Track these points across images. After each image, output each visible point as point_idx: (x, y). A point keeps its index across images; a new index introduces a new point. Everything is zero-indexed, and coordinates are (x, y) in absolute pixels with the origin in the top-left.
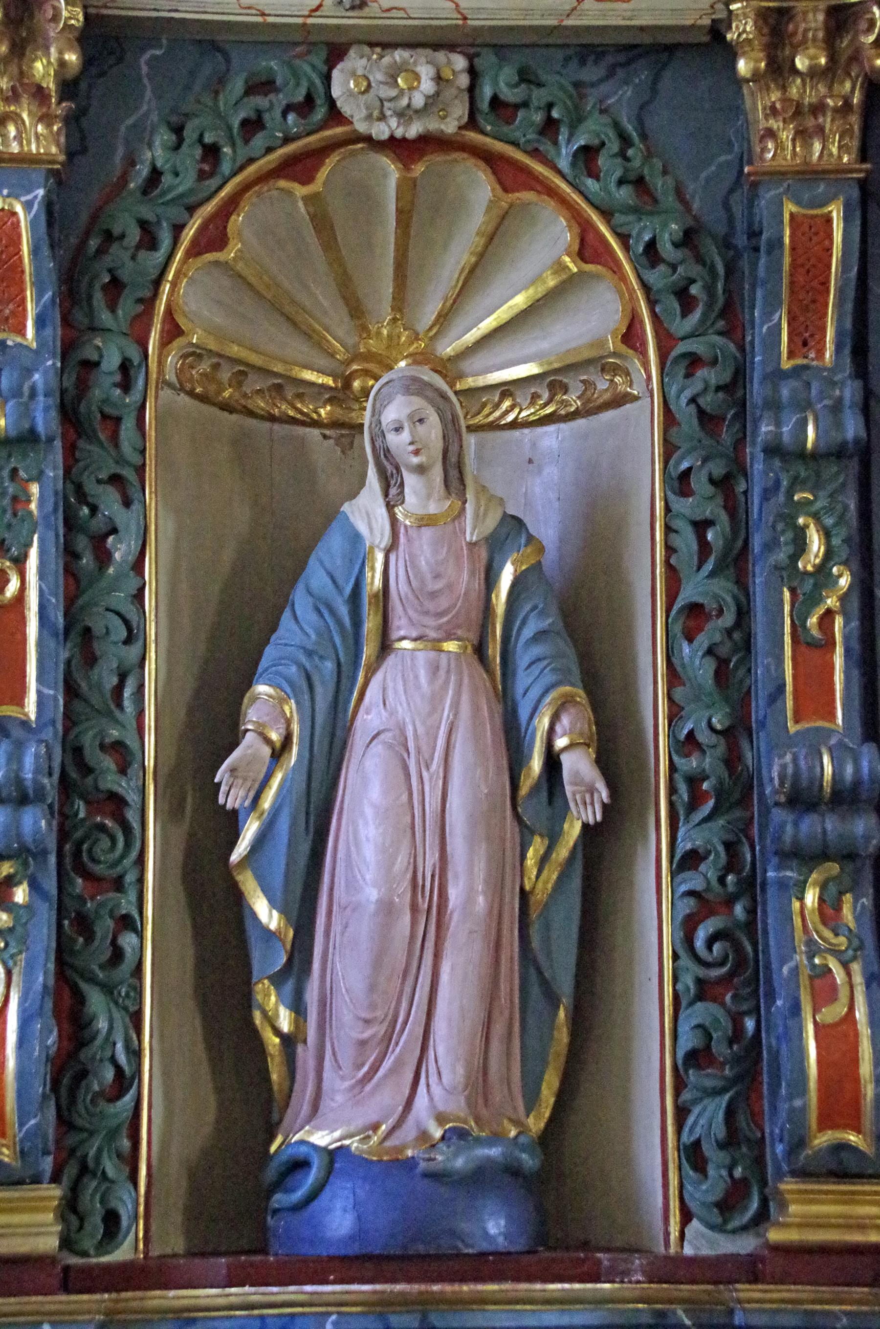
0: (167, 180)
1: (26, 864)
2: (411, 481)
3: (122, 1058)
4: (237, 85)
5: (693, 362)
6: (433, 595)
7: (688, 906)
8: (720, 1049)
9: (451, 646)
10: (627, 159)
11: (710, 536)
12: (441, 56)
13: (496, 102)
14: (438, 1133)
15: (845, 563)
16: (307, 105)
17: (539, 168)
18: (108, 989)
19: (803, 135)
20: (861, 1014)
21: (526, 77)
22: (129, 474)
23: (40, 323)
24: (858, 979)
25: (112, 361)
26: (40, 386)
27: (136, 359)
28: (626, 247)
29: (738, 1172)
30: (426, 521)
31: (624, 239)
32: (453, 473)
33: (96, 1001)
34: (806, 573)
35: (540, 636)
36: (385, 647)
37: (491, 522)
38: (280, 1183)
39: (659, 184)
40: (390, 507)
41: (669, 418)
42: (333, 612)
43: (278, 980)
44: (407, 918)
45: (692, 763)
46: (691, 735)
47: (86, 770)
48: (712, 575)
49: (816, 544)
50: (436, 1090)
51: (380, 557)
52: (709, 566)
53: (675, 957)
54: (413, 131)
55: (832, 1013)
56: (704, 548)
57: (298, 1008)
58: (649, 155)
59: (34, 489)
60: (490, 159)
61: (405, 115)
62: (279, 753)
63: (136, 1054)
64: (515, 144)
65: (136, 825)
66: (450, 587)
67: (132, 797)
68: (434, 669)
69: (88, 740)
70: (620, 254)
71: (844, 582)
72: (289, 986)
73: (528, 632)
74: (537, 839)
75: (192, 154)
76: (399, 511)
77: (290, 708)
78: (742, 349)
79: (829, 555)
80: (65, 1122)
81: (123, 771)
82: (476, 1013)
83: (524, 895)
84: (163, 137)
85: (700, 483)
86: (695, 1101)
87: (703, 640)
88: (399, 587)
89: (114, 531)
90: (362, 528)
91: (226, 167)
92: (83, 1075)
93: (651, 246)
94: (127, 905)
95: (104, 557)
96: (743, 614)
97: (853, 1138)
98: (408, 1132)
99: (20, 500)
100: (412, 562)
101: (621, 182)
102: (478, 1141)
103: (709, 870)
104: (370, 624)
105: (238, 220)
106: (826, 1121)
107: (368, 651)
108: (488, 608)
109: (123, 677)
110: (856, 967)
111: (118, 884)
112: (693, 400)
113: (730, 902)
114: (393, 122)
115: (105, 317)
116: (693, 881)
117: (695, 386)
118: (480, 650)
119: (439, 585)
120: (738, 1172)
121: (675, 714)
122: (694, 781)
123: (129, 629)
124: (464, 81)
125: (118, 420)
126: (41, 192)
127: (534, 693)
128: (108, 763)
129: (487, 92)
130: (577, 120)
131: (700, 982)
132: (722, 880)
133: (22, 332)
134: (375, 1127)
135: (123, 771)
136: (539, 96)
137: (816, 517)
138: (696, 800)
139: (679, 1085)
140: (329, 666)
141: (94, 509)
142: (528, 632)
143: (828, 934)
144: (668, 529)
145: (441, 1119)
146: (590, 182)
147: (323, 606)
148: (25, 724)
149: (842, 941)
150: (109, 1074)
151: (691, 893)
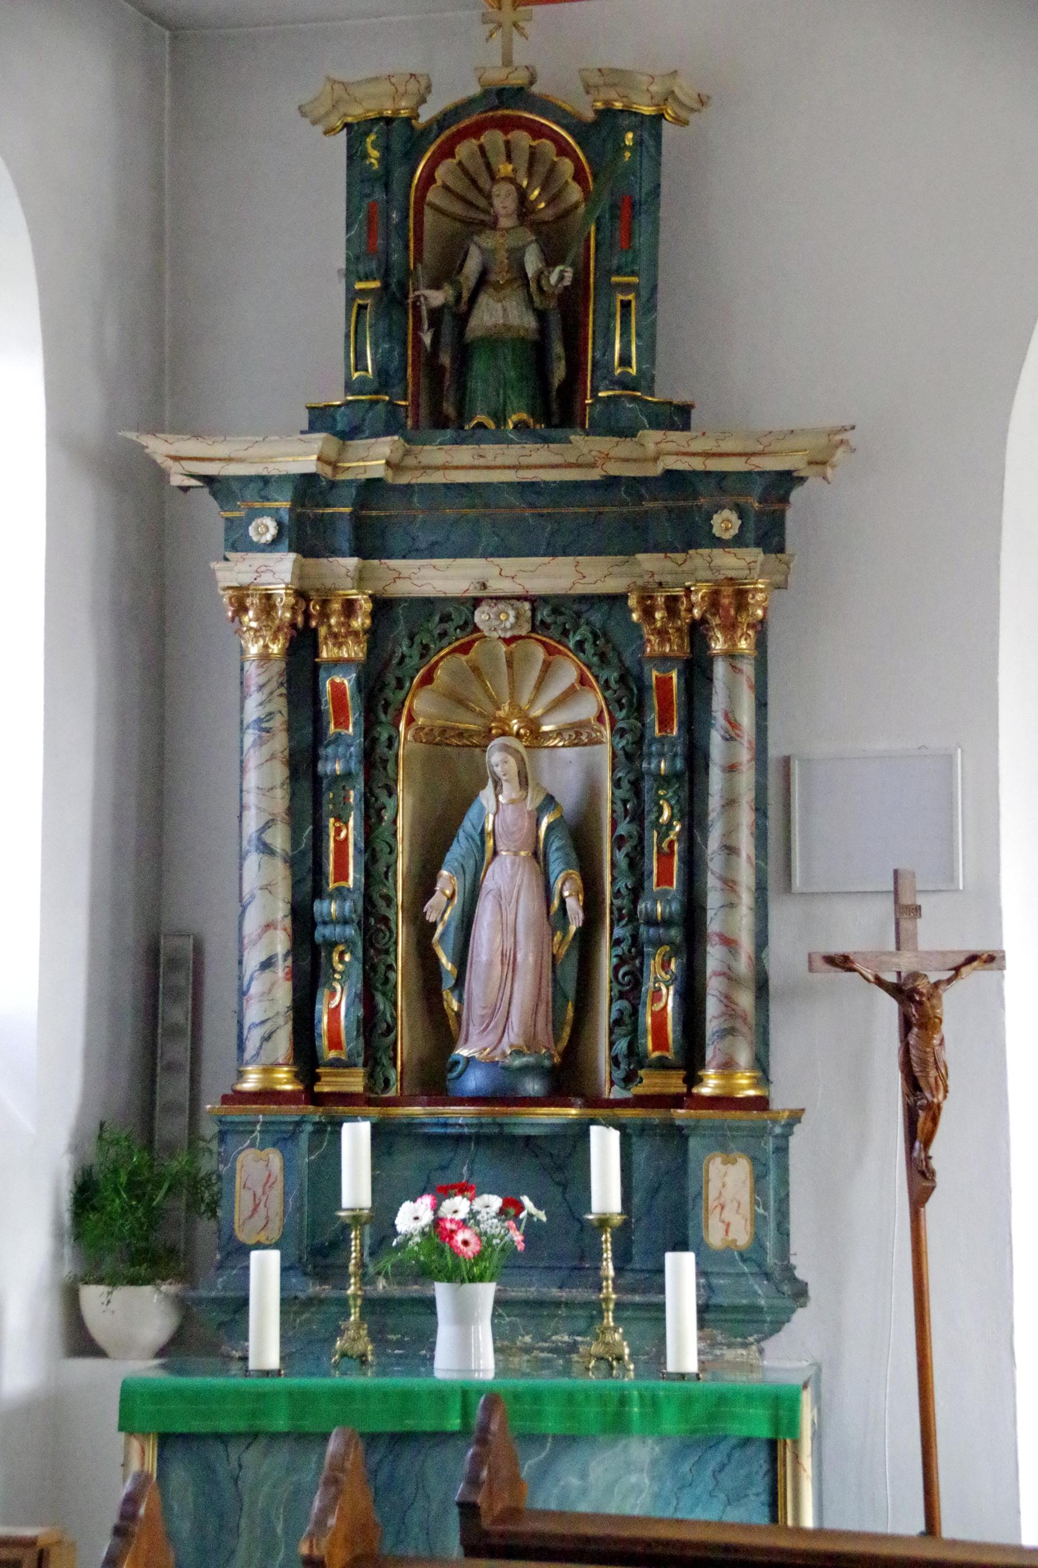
0: (407, 660)
1: (348, 947)
2: (505, 785)
3: (389, 1019)
5: (622, 733)
6: (513, 833)
7: (615, 960)
8: (627, 1019)
9: (523, 853)
10: (597, 645)
11: (628, 806)
13: (542, 622)
14: (509, 1052)
15: (679, 820)
16: (462, 627)
17: (561, 648)
18: (384, 994)
19: (662, 644)
21: (556, 611)
22: (391, 783)
23: (355, 724)
24: (671, 992)
25: (384, 736)
26: (354, 754)
27: (395, 735)
28: (597, 681)
29: (632, 1067)
30: (512, 802)
31: (596, 677)
32: (524, 780)
33: (379, 998)
34: (662, 825)
35: (557, 849)
36: (495, 853)
37: (539, 800)
38: (450, 1071)
39: (611, 655)
40: (497, 796)
42: (473, 840)
43: (452, 989)
44: (499, 967)
45: (618, 902)
46: (619, 890)
47: (374, 906)
48: (629, 823)
50: (512, 1035)
51: (491, 817)
52: (628, 819)
53: (611, 982)
54: (508, 635)
55: (658, 1007)
56: (626, 810)
57: (460, 1000)
58: (608, 641)
59: (352, 793)
60: (544, 643)
61: (505, 630)
62: (451, 898)
63: (395, 1019)
64: (551, 638)
65: (393, 927)
66: (520, 830)
67: (392, 917)
68: (513, 863)
69: (376, 896)
70: (595, 684)
71: (678, 828)
72: (457, 992)
73: (554, 847)
74: (558, 933)
75: (416, 652)
76: (500, 798)
77: (455, 881)
78: (643, 725)
79: (672, 817)
80: (368, 1044)
81: (388, 906)
82: (529, 1004)
84: (405, 642)
86: (617, 1039)
88: (499, 830)
89: (385, 807)
90: (485, 803)
91: (432, 652)
92: (375, 1026)
93: (607, 681)
94: (390, 960)
95: (381, 819)
96: (641, 839)
97: (667, 1054)
98: (499, 1051)
99: (346, 798)
100: (504, 820)
101: (595, 654)
102: (524, 1055)
103: (625, 946)
104: (490, 843)
105: (439, 672)
107: (488, 855)
108: (537, 837)
109: (388, 867)
110: (671, 988)
111: (387, 952)
112: (623, 747)
113: (634, 958)
114: (500, 632)
116: (619, 951)
117: (624, 742)
118: (535, 854)
119: (515, 829)
120: (632, 1067)
121: (614, 880)
122: (620, 909)
123: (390, 846)
124: (529, 614)
125: (387, 761)
126: (354, 675)
127: (555, 874)
129: (539, 617)
130: (576, 627)
131: (620, 992)
132: (630, 951)
133: (347, 728)
134: (485, 1049)
135: (388, 906)
136: (561, 619)
137: (667, 800)
138: (621, 918)
140: (472, 862)
141: (377, 799)
142: (554, 847)
143: (663, 974)
144: (613, 803)
145: (511, 1046)
146: (581, 654)
147: (469, 837)
148: (349, 889)
149: (668, 977)
150: (385, 1026)
151: (616, 956)
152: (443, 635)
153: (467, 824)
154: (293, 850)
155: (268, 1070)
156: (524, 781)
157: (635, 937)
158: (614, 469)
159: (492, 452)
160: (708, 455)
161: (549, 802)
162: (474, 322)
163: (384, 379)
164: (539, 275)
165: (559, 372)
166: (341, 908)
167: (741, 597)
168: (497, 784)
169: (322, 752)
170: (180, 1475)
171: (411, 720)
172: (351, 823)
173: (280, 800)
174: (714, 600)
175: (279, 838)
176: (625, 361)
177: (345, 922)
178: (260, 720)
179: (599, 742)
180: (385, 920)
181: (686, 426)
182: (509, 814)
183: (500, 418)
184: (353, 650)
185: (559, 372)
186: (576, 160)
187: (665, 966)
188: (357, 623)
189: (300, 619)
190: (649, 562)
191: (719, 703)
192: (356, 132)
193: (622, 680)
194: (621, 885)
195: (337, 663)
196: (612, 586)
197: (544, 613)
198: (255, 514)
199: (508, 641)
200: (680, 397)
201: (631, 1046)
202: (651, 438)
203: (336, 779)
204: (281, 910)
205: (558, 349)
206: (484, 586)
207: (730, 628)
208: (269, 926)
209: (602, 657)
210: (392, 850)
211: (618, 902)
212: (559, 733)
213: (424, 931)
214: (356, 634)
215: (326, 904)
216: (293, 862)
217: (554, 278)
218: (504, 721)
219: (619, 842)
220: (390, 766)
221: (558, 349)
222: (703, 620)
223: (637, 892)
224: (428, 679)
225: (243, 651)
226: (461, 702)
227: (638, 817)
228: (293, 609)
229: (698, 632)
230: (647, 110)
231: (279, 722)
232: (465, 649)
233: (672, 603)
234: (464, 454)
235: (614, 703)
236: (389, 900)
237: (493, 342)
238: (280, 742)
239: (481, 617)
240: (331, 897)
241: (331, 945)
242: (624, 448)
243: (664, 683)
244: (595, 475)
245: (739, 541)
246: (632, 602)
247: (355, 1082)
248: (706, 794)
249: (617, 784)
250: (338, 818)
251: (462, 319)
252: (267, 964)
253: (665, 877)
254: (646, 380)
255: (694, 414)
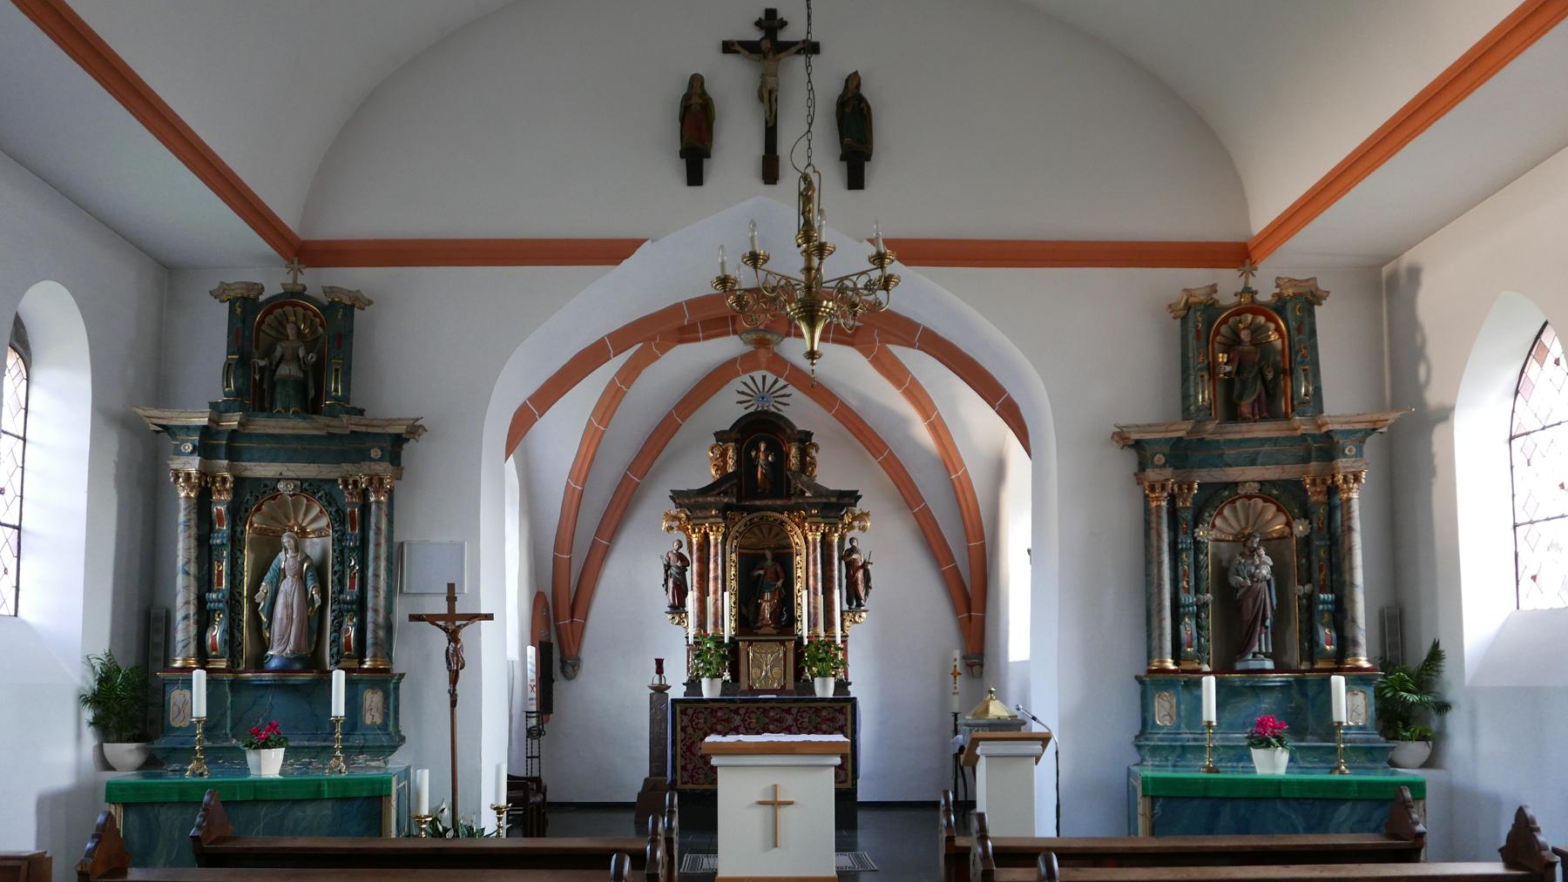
4: (262, 486)
5: (337, 532)
12: (296, 482)
19: (352, 498)
20: (352, 636)
21: (310, 485)
25: (239, 530)
30: (292, 557)
36: (285, 577)
41: (333, 540)
45: (334, 596)
49: (353, 563)
57: (270, 633)
61: (290, 491)
62: (266, 593)
75: (253, 498)
83: (309, 617)
85: (337, 551)
87: (337, 576)
94: (241, 617)
96: (343, 572)
105: (263, 507)
106: (347, 651)
115: (239, 523)
118: (301, 577)
128: (237, 595)
139: (331, 645)
147: (274, 570)
152: (265, 492)
153: (273, 565)
154: (199, 573)
155: (184, 660)
156: (297, 549)
157: (340, 611)
158: (332, 430)
159: (282, 422)
160: (367, 426)
161: (307, 557)
162: (278, 373)
163: (239, 392)
164: (304, 357)
165: (312, 393)
166: (218, 596)
167: (381, 481)
168: (286, 549)
169: (212, 535)
170: (133, 817)
171: (251, 525)
172: (224, 564)
173: (193, 555)
174: (370, 482)
175: (193, 569)
176: (336, 390)
177: (219, 601)
178: (185, 522)
179: (329, 535)
180: (239, 602)
181: (362, 415)
182: (291, 561)
183: (287, 410)
184: (225, 497)
185: (312, 393)
186: (320, 318)
187: (351, 620)
188: (228, 485)
189: (203, 483)
190: (347, 467)
191: (373, 520)
192: (232, 303)
193: (337, 511)
194: (335, 589)
195: (219, 502)
196: (332, 476)
197: (306, 485)
198: (187, 441)
199: (291, 496)
200: (359, 406)
201: (338, 650)
202: (345, 418)
203: (217, 545)
204: (192, 597)
205: (311, 384)
206: (281, 474)
207: (377, 492)
208: (187, 603)
209: (330, 504)
210: (242, 574)
211: (334, 596)
212: (313, 532)
213: (254, 607)
214: (227, 490)
215: (211, 594)
216: (199, 579)
217: (310, 357)
218: (293, 527)
219: (334, 573)
220: (242, 542)
221: (311, 384)
222: (367, 489)
223: (341, 592)
224: (259, 509)
225: (179, 494)
226: (274, 519)
227: (342, 563)
228: (199, 479)
229: (365, 494)
230: (349, 303)
231: (193, 523)
232: (274, 498)
233: (355, 482)
234: (272, 422)
235: (333, 521)
236: (241, 594)
237: (284, 381)
238: (193, 531)
239: (281, 486)
240: (215, 592)
241: (215, 611)
242: (335, 422)
243: (352, 513)
244: (323, 433)
245: (381, 459)
246: (340, 481)
247: (223, 665)
248: (368, 555)
249: (334, 551)
250: (219, 562)
251: (275, 371)
252: (186, 617)
253: (352, 586)
254: (346, 398)
255: (366, 413)
